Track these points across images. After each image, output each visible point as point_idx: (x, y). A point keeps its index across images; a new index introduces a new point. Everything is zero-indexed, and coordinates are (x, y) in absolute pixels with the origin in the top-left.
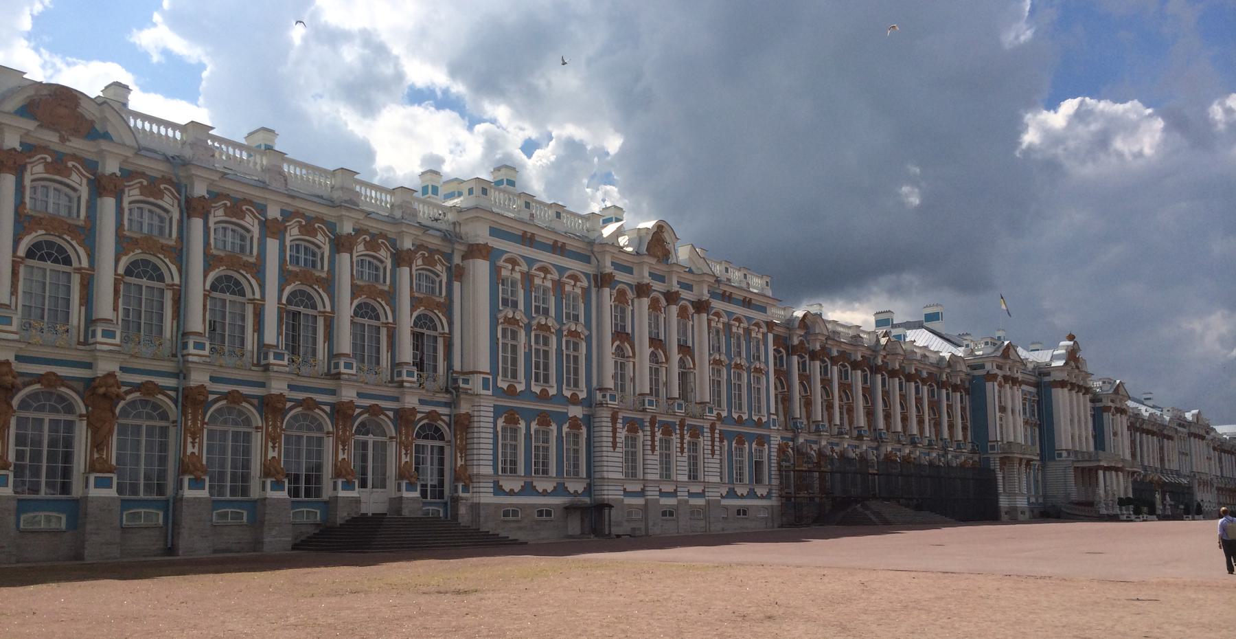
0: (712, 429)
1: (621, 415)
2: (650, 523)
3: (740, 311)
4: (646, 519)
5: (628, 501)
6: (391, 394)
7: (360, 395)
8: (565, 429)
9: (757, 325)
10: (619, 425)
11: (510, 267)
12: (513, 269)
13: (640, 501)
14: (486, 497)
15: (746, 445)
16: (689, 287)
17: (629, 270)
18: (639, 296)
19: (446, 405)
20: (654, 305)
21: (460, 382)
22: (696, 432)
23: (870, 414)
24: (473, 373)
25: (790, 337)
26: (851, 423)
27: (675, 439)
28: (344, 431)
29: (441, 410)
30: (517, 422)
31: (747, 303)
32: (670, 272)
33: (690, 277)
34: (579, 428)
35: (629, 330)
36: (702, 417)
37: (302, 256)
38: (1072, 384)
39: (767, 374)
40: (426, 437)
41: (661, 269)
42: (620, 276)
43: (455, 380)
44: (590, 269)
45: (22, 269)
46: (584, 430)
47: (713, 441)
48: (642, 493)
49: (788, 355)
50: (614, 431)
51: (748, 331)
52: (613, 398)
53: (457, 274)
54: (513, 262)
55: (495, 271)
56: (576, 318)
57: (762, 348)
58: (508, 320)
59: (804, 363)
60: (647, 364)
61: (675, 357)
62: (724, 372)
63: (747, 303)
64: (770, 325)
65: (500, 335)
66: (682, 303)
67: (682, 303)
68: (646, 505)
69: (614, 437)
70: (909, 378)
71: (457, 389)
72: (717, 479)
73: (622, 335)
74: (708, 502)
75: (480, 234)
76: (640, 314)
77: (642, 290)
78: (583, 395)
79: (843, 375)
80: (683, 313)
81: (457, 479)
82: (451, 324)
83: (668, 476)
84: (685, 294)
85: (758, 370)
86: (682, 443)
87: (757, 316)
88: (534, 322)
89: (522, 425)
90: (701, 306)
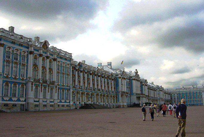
0: (56, 87)
3: (64, 61)
5: (35, 103)
12: (9, 49)
16: (52, 55)
17: (38, 51)
18: (40, 57)
20: (43, 60)
23: (94, 85)
27: (47, 89)
38: (136, 80)
46: (25, 87)
50: (32, 87)
69: (32, 88)
70: (103, 77)
72: (57, 98)
77: (41, 55)
79: (88, 76)
85: (68, 75)
90: (55, 60)
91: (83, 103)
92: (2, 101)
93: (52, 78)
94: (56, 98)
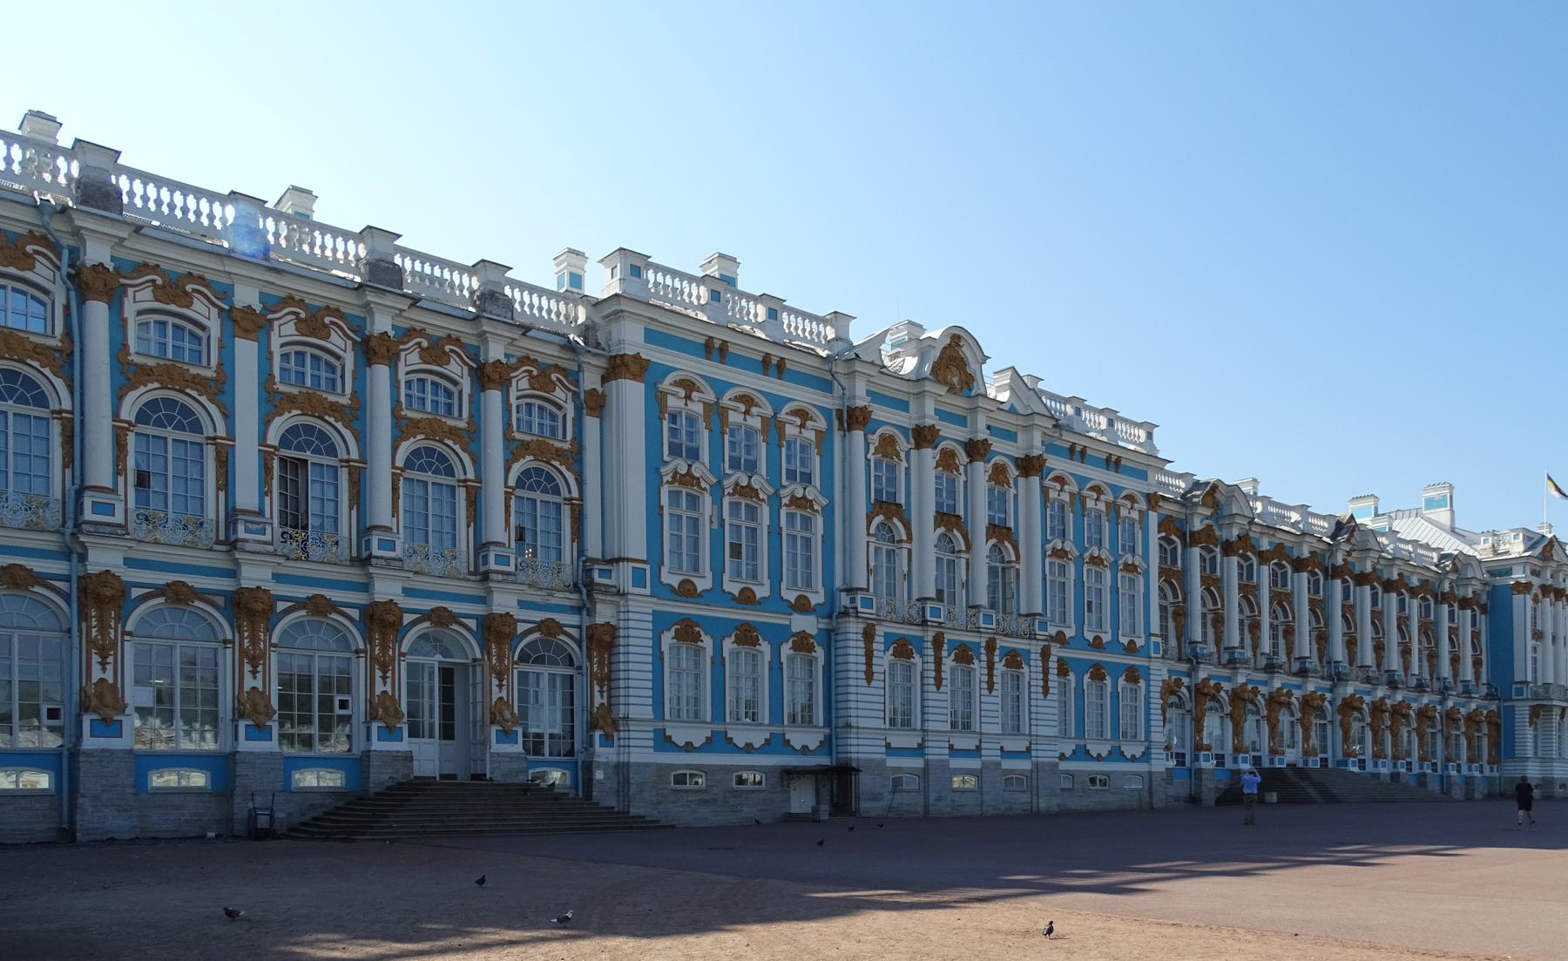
0: (1045, 654)
1: (880, 630)
6: (567, 603)
7: (407, 592)
8: (786, 650)
10: (878, 645)
15: (1108, 681)
16: (1010, 436)
19: (577, 610)
20: (947, 461)
21: (596, 575)
22: (1014, 660)
23: (1322, 638)
24: (623, 559)
26: (1289, 651)
28: (384, 649)
29: (563, 618)
30: (697, 638)
34: (811, 649)
35: (902, 500)
36: (1032, 636)
37: (429, 397)
39: (1146, 574)
40: (539, 661)
42: (879, 413)
43: (588, 572)
45: (131, 439)
46: (819, 653)
47: (1046, 671)
49: (1184, 546)
50: (869, 655)
51: (1113, 508)
52: (868, 603)
53: (596, 404)
56: (807, 479)
57: (1139, 534)
58: (739, 490)
60: (931, 554)
61: (983, 546)
62: (1072, 568)
64: (1153, 500)
69: (869, 664)
70: (1389, 586)
71: (590, 585)
73: (887, 507)
74: (1037, 767)
76: (921, 479)
77: (923, 436)
78: (817, 598)
79: (1278, 579)
83: (967, 726)
84: (998, 445)
85: (1130, 568)
86: (991, 675)
89: (707, 642)
93: (966, 585)
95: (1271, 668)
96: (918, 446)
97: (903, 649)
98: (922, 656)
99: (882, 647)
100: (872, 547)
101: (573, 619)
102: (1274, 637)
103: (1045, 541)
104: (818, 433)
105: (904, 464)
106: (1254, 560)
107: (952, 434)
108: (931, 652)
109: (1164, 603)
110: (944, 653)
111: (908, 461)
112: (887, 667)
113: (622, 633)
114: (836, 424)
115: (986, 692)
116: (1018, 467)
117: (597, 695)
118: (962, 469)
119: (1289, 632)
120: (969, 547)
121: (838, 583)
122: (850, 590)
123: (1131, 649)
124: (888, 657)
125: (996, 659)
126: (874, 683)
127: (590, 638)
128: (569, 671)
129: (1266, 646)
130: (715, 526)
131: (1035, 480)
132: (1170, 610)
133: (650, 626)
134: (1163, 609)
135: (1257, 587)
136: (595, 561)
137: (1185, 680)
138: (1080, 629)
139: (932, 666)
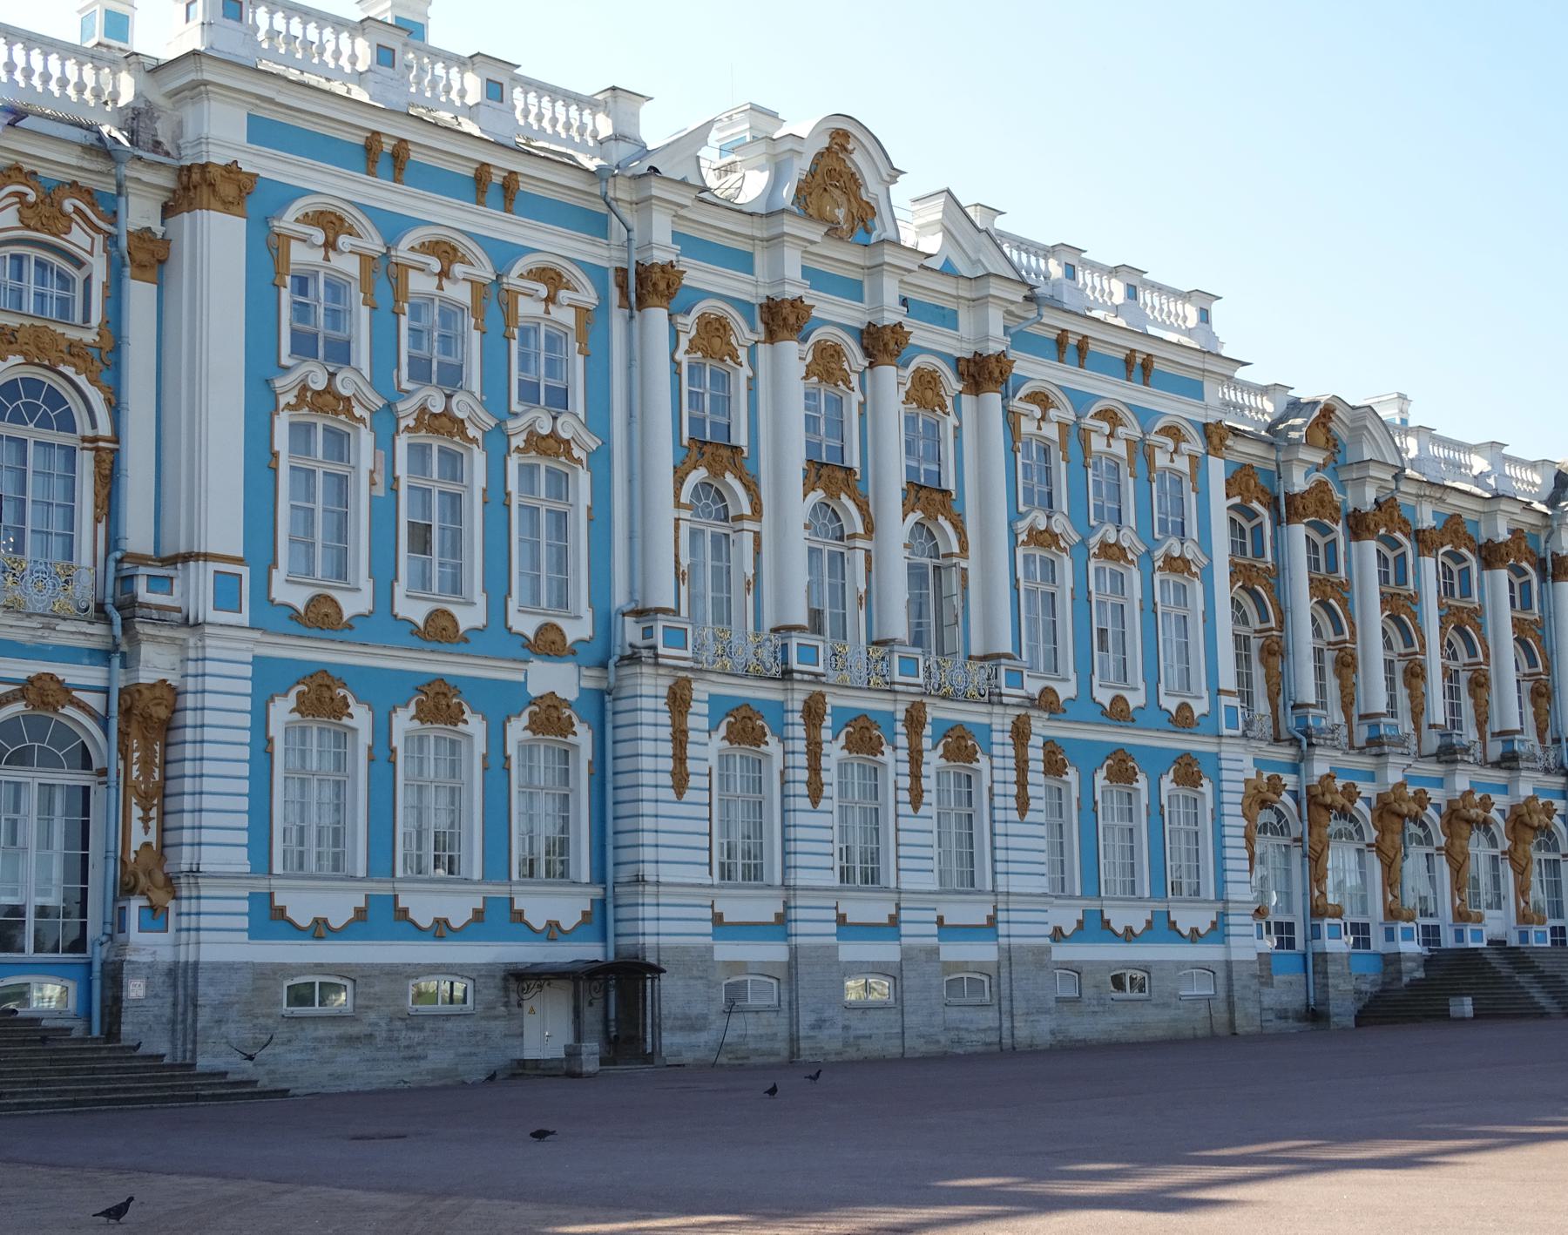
0: (1020, 733)
1: (701, 691)
2: (806, 1019)
3: (1114, 391)
4: (793, 1005)
5: (726, 951)
8: (517, 731)
9: (1173, 432)
10: (697, 720)
11: (319, 236)
12: (330, 245)
13: (776, 952)
14: (221, 939)
15: (1142, 783)
16: (945, 318)
17: (744, 262)
20: (826, 364)
22: (961, 745)
24: (187, 558)
25: (1278, 474)
26: (1481, 722)
29: (70, 674)
30: (339, 710)
31: (1138, 367)
32: (876, 269)
33: (946, 286)
34: (565, 728)
35: (741, 438)
36: (993, 698)
41: (844, 257)
43: (127, 580)
44: (603, 254)
46: (583, 737)
47: (1022, 767)
48: (782, 924)
49: (1277, 522)
50: (680, 738)
51: (1142, 451)
52: (677, 637)
54: (331, 224)
55: (269, 251)
56: (559, 399)
57: (1191, 499)
58: (429, 421)
59: (1332, 546)
60: (799, 542)
62: (1066, 565)
63: (1138, 367)
65: (282, 442)
66: (919, 361)
67: (919, 361)
68: (792, 965)
69: (680, 757)
71: (129, 607)
72: (1040, 885)
73: (714, 452)
75: (221, 134)
76: (778, 399)
77: (780, 318)
78: (578, 629)
80: (924, 388)
81: (127, 888)
82: (116, 408)
83: (871, 877)
84: (921, 334)
85: (1177, 565)
86: (916, 776)
87: (1173, 408)
88: (406, 407)
89: (360, 718)
90: (980, 373)
91: (1412, 947)
92: (255, 933)
93: (866, 600)
94: (1017, 884)
95: (1448, 754)
96: (772, 337)
97: (745, 726)
98: (783, 739)
99: (704, 723)
100: (685, 528)
101: (93, 675)
102: (1452, 693)
103: (1015, 516)
104: (581, 311)
105: (745, 371)
106: (1408, 546)
107: (835, 315)
108: (800, 731)
109: (1243, 630)
110: (826, 734)
111: (753, 364)
112: (714, 762)
113: (190, 701)
114: (615, 294)
115: (906, 809)
116: (961, 376)
117: (136, 826)
118: (854, 379)
119: (1479, 684)
120: (870, 529)
121: (620, 599)
122: (640, 613)
123: (1183, 720)
124: (718, 742)
125: (927, 743)
126: (689, 795)
127: (126, 713)
128: (82, 779)
129: (1438, 711)
130: (380, 491)
131: (994, 399)
132: (1255, 644)
133: (247, 687)
134: (1241, 642)
135: (1415, 599)
136: (140, 560)
137: (1289, 780)
138: (1085, 684)
139: (802, 760)
